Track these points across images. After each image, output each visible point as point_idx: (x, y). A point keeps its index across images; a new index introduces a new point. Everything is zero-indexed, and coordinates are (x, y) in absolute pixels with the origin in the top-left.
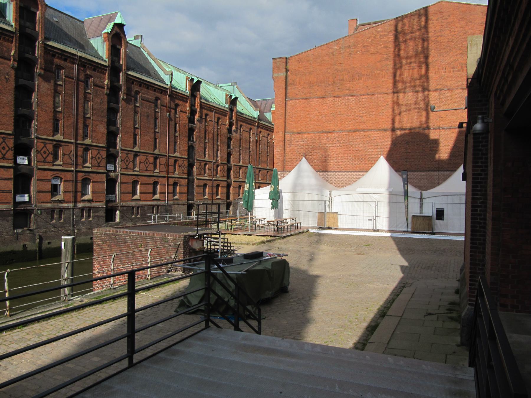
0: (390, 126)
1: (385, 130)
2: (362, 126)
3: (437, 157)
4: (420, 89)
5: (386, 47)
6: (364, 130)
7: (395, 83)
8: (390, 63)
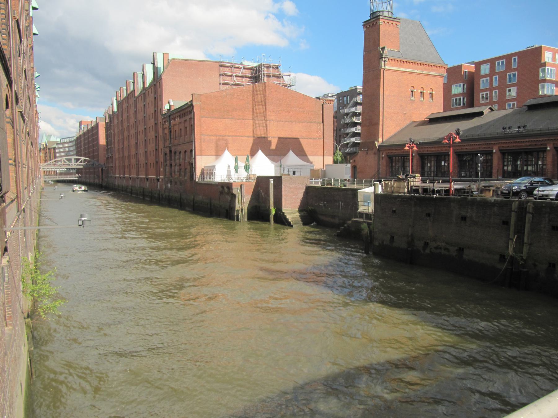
0: (252, 135)
1: (248, 137)
2: (238, 134)
3: (271, 148)
4: (263, 118)
5: (247, 98)
6: (239, 136)
7: (253, 114)
8: (250, 106)
